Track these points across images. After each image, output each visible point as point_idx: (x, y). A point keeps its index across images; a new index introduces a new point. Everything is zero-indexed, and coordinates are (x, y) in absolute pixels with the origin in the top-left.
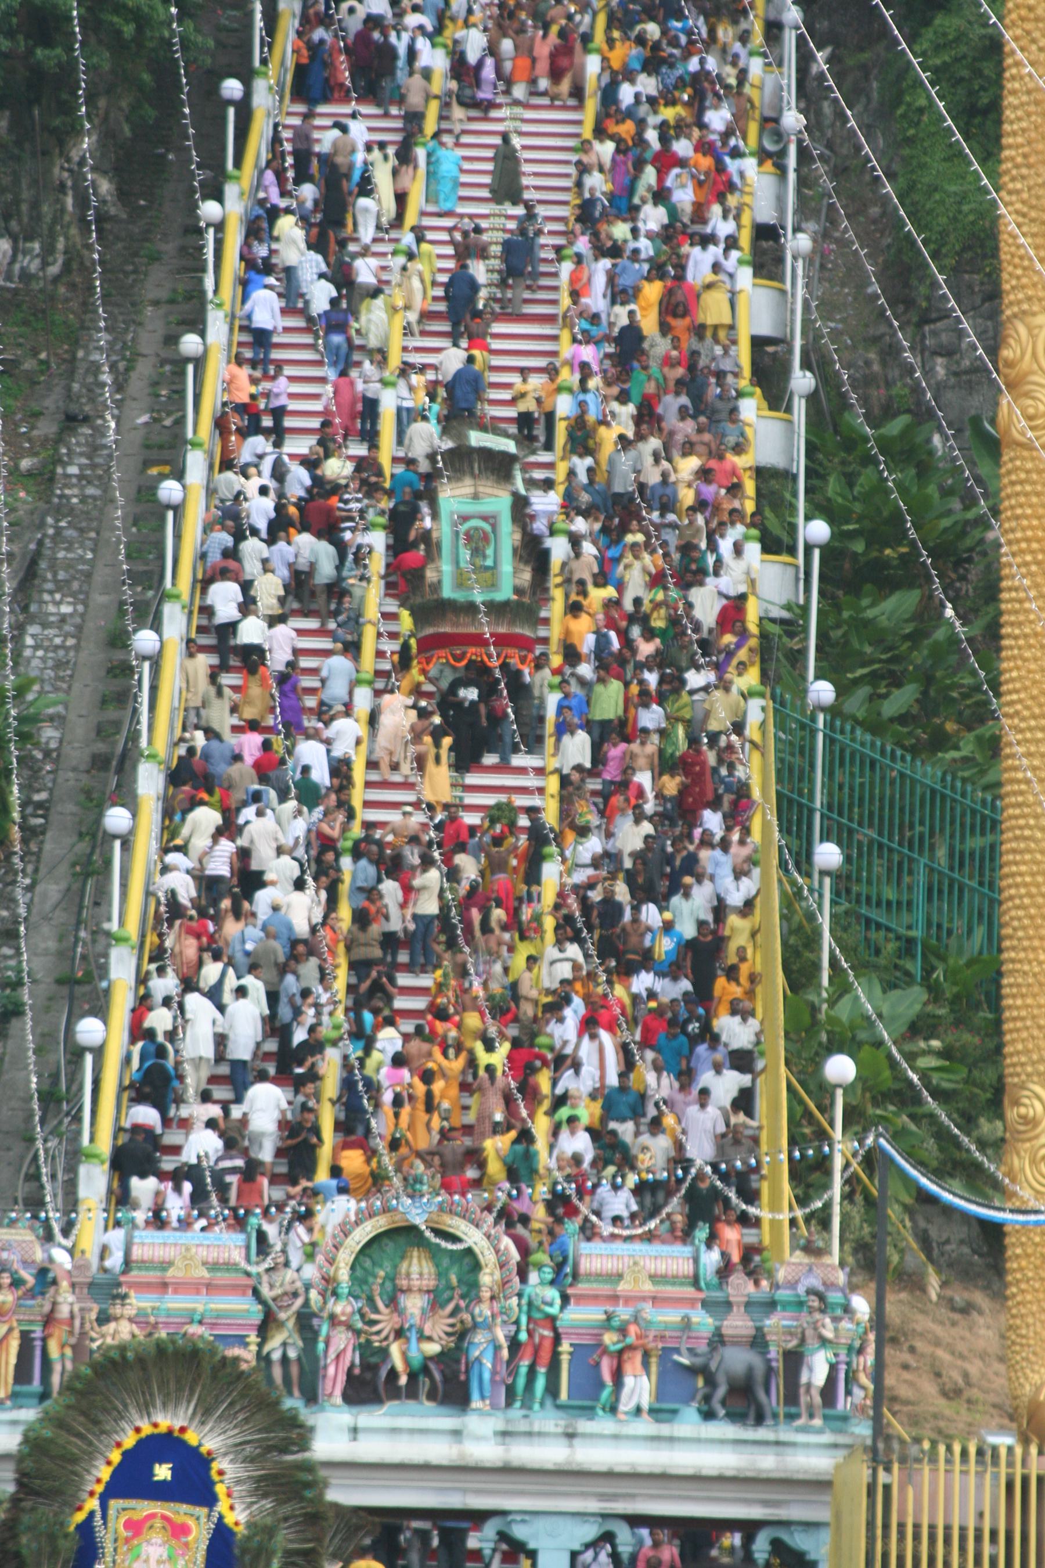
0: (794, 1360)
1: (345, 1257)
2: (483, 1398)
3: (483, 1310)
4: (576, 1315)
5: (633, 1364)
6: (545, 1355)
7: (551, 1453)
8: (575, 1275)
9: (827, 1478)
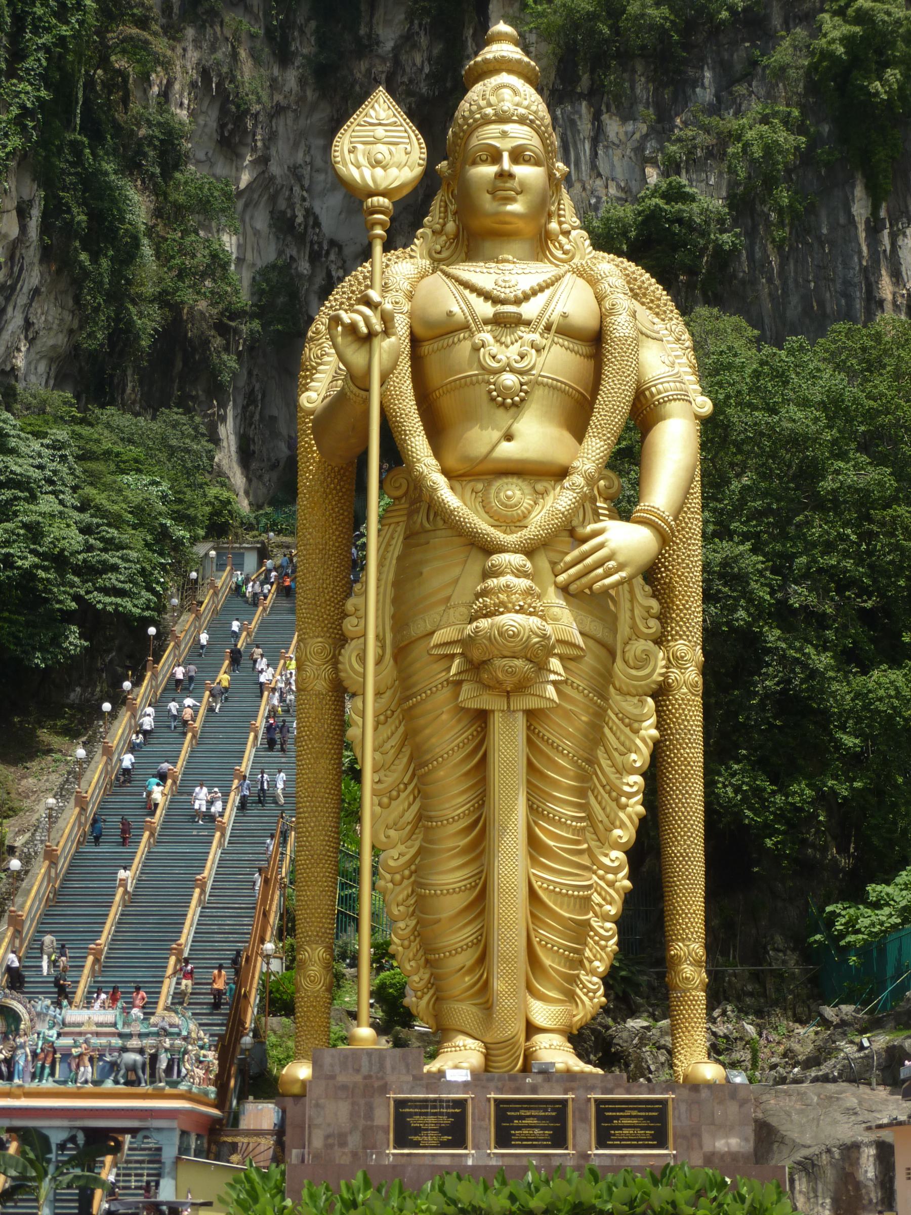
0: (154, 1058)
4: (67, 1041)
6: (49, 1059)
8: (64, 1024)
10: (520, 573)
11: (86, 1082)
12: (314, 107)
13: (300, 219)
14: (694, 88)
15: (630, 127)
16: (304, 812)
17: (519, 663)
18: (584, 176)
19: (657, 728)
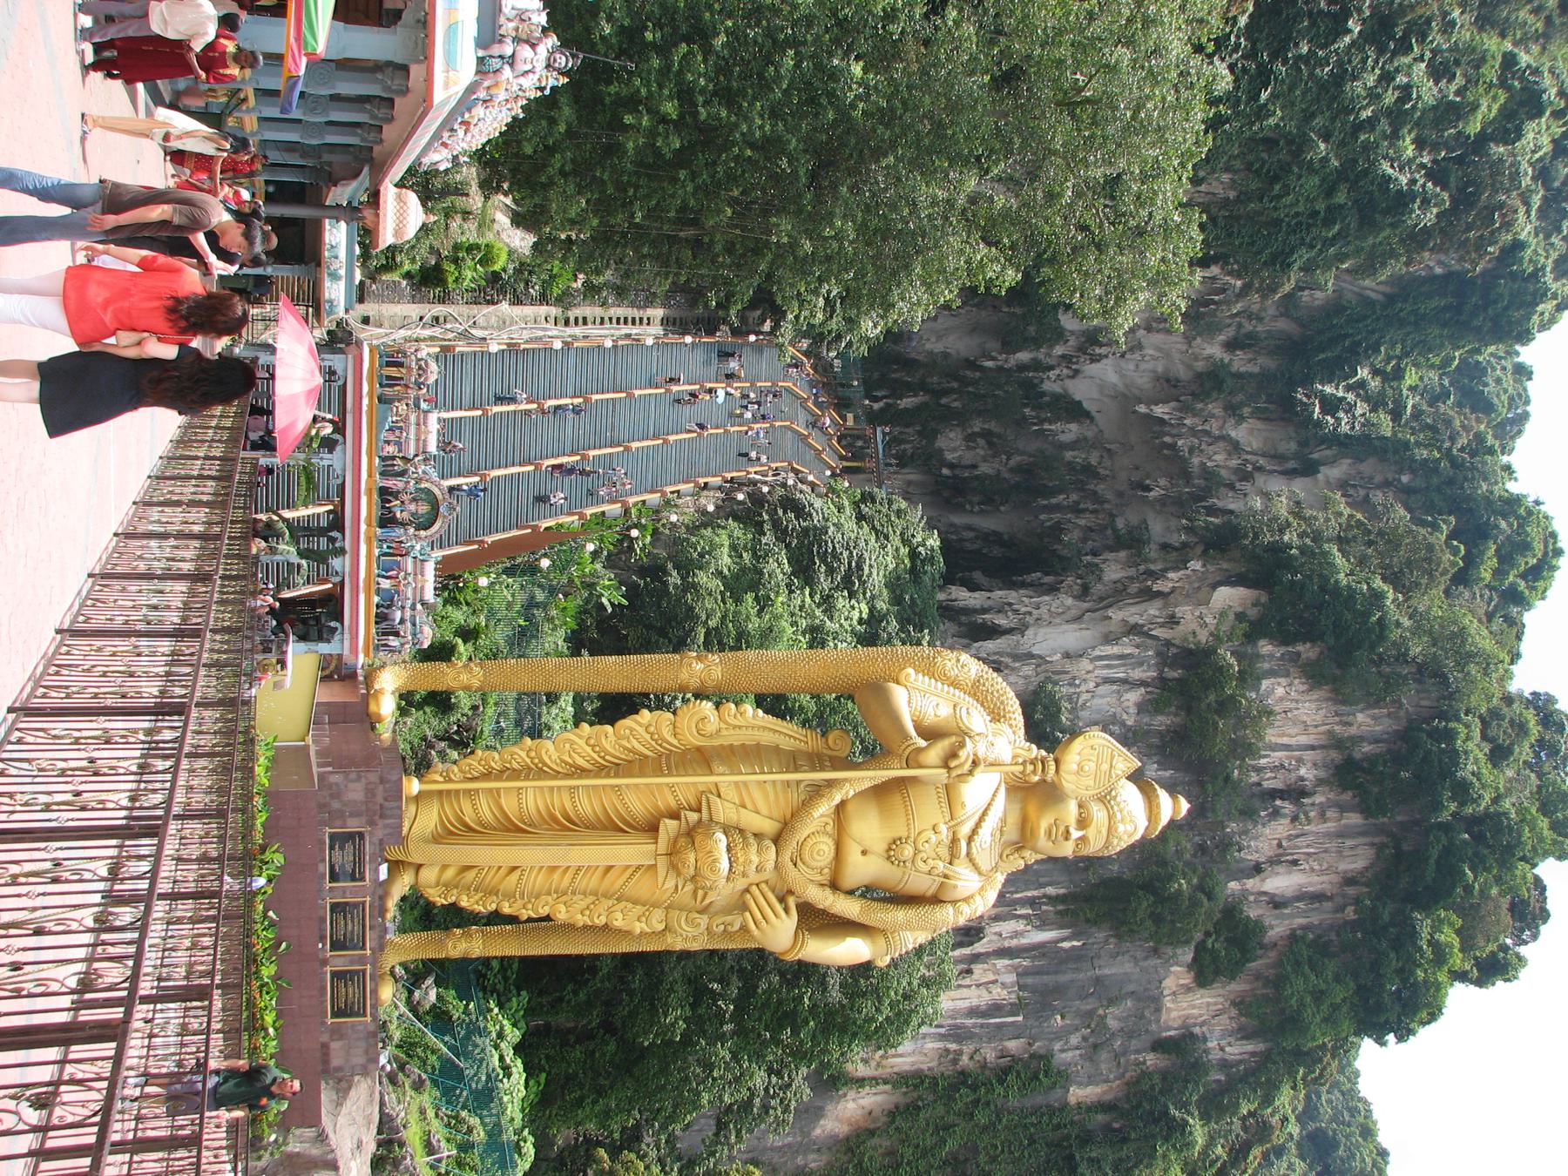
0: (397, 634)
1: (427, 485)
10: (759, 870)
12: (1189, 367)
13: (1098, 351)
14: (1158, 762)
15: (1133, 710)
17: (692, 872)
18: (1097, 672)
19: (643, 934)
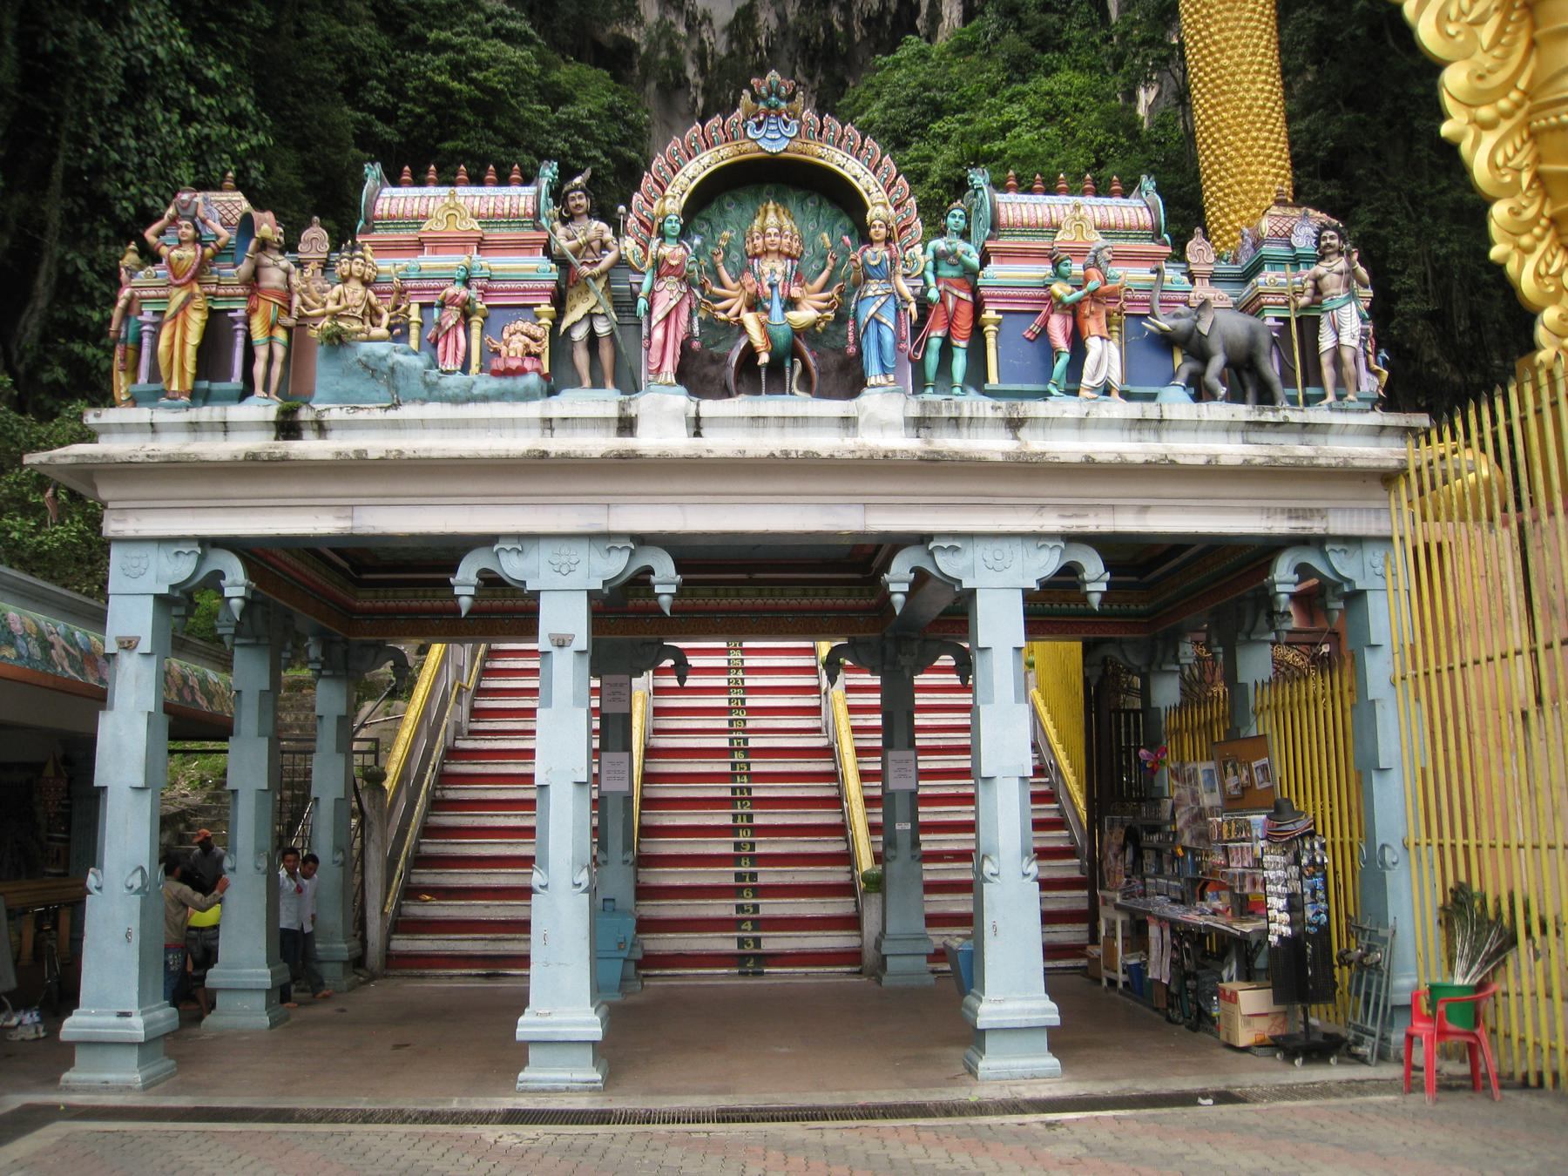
2: (884, 370)
3: (876, 254)
5: (1094, 326)
6: (964, 322)
7: (993, 445)
8: (995, 225)
9: (1393, 464)
11: (1107, 390)
16: (1221, 31)
